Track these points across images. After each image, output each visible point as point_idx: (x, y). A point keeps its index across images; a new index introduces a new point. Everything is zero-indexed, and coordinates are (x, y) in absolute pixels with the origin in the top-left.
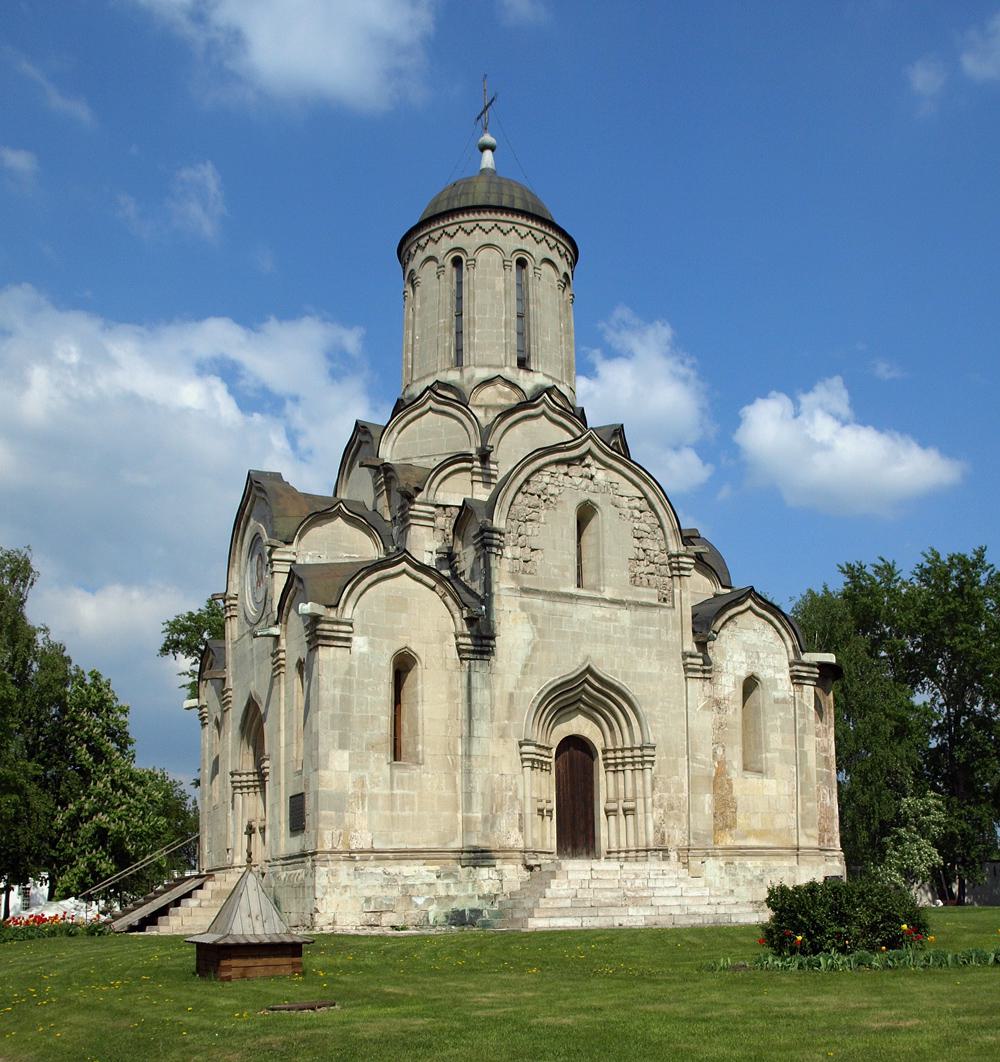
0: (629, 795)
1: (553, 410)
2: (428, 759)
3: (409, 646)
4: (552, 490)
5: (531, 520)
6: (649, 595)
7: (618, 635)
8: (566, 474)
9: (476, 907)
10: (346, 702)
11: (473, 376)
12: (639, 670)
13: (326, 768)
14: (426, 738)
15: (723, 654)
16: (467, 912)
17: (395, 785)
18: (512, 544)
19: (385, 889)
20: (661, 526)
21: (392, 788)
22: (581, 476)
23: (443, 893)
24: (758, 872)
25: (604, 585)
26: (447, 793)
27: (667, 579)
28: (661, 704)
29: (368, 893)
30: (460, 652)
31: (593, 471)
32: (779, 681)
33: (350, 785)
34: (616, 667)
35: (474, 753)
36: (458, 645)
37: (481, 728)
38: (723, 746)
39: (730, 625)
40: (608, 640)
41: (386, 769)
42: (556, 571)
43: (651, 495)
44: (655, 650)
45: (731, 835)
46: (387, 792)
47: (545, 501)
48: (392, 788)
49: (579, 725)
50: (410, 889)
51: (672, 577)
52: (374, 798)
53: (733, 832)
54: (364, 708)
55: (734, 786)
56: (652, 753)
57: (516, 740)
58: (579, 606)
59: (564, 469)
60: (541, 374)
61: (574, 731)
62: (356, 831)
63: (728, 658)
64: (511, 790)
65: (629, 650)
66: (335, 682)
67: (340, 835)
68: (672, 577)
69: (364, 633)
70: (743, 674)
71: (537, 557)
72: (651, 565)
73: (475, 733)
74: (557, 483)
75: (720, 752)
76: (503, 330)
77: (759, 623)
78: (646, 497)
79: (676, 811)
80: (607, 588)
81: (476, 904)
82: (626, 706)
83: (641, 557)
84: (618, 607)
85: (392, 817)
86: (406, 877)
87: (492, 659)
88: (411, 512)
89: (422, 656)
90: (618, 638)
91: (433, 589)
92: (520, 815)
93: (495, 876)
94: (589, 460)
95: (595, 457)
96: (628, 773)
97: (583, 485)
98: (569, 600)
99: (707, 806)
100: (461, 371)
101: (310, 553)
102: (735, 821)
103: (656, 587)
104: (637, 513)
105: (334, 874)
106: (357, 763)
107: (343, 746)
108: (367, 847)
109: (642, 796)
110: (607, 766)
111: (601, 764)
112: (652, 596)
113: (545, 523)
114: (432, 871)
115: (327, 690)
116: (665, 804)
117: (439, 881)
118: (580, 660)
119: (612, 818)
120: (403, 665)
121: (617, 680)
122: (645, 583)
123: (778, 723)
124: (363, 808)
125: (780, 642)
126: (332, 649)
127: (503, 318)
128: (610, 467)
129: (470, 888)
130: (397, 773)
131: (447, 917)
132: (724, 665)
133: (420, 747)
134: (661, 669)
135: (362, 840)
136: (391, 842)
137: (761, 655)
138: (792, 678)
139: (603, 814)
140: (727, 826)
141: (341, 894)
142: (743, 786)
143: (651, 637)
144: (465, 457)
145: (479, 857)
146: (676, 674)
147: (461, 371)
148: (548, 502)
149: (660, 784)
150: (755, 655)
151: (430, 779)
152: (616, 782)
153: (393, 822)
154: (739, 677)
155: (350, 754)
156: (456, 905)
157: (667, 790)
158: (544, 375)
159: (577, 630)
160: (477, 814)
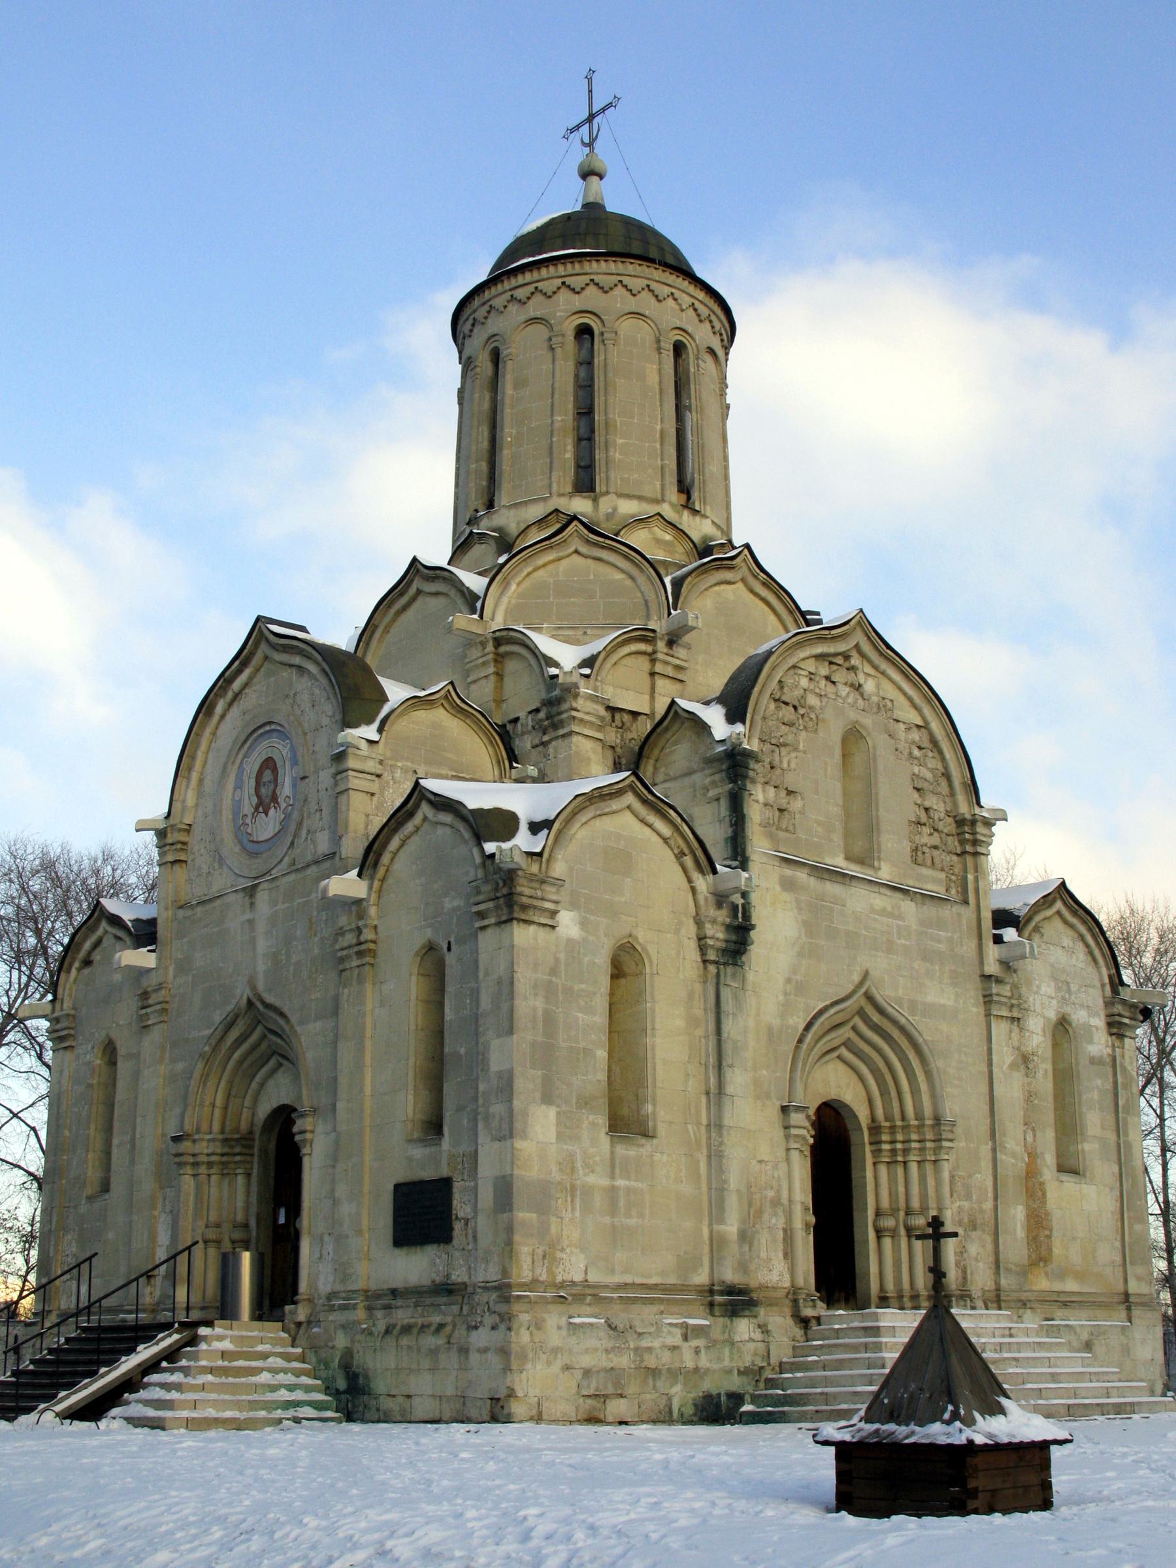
0: (915, 1204)
1: (756, 577)
2: (662, 1129)
3: (634, 932)
4: (812, 700)
5: (785, 745)
6: (932, 881)
7: (903, 941)
8: (827, 678)
9: (734, 1389)
10: (549, 1021)
11: (615, 509)
12: (930, 999)
13: (524, 1136)
14: (659, 1092)
15: (1029, 983)
16: (723, 1398)
17: (617, 1171)
18: (763, 780)
19: (611, 1355)
20: (947, 775)
21: (613, 1177)
22: (846, 684)
23: (689, 1361)
24: (1085, 1336)
25: (879, 859)
26: (686, 1188)
27: (955, 858)
28: (956, 1056)
29: (587, 1361)
30: (703, 949)
31: (861, 678)
32: (1094, 1030)
33: (554, 1168)
34: (901, 992)
35: (727, 1121)
36: (701, 938)
37: (738, 1080)
38: (1033, 1130)
40: (890, 948)
41: (604, 1141)
42: (820, 829)
43: (935, 726)
45: (1047, 1274)
46: (605, 1182)
47: (803, 716)
48: (613, 1177)
49: (837, 1082)
50: (646, 1356)
51: (964, 853)
52: (588, 1191)
53: (1048, 1269)
54: (573, 1033)
55: (1049, 1195)
56: (950, 1136)
57: (778, 1104)
58: (853, 890)
59: (824, 670)
60: (708, 522)
61: (832, 1094)
62: (563, 1250)
63: (1035, 989)
64: (772, 1188)
65: (916, 966)
66: (535, 986)
67: (544, 1256)
68: (964, 853)
69: (573, 906)
70: (1052, 1015)
71: (796, 804)
72: (936, 834)
73: (730, 1089)
74: (817, 690)
75: (1030, 1139)
76: (658, 446)
77: (1067, 938)
78: (924, 727)
79: (979, 1232)
80: (882, 863)
81: (735, 1383)
82: (911, 1055)
83: (924, 818)
84: (899, 895)
85: (613, 1226)
86: (640, 1334)
87: (744, 958)
88: (574, 713)
89: (652, 950)
91: (665, 840)
92: (785, 1230)
93: (758, 1335)
94: (855, 661)
95: (862, 655)
96: (913, 1167)
97: (850, 700)
98: (839, 879)
99: (1019, 1226)
100: (595, 500)
101: (399, 764)
102: (1050, 1250)
103: (942, 870)
104: (916, 752)
105: (539, 1325)
106: (567, 1130)
107: (547, 1098)
108: (578, 1278)
109: (934, 1206)
110: (877, 1153)
111: (868, 1149)
112: (936, 881)
113: (805, 752)
114: (675, 1325)
115: (525, 998)
116: (966, 1220)
117: (686, 1344)
118: (856, 978)
119: (887, 1242)
120: (625, 965)
121: (904, 1016)
122: (929, 862)
123: (1096, 1095)
124: (573, 1210)
125: (1091, 969)
126: (532, 928)
127: (658, 427)
128: (883, 673)
129: (727, 1358)
130: (621, 1150)
131: (696, 1405)
132: (1031, 999)
133: (650, 1108)
134: (956, 1001)
135: (573, 1267)
136: (613, 1272)
137: (1074, 988)
138: (1110, 1025)
139: (872, 1235)
140: (1041, 1259)
141: (549, 1363)
142: (1062, 1194)
143: (942, 947)
144: (646, 636)
145: (735, 1301)
146: (975, 1010)
147: (595, 500)
148: (806, 719)
149: (959, 1186)
150: (1065, 987)
151: (667, 1161)
152: (892, 1181)
153: (615, 1235)
154: (1049, 1019)
155: (558, 1113)
156: (709, 1385)
157: (968, 1196)
158: (713, 522)
159: (851, 928)
160: (731, 1228)
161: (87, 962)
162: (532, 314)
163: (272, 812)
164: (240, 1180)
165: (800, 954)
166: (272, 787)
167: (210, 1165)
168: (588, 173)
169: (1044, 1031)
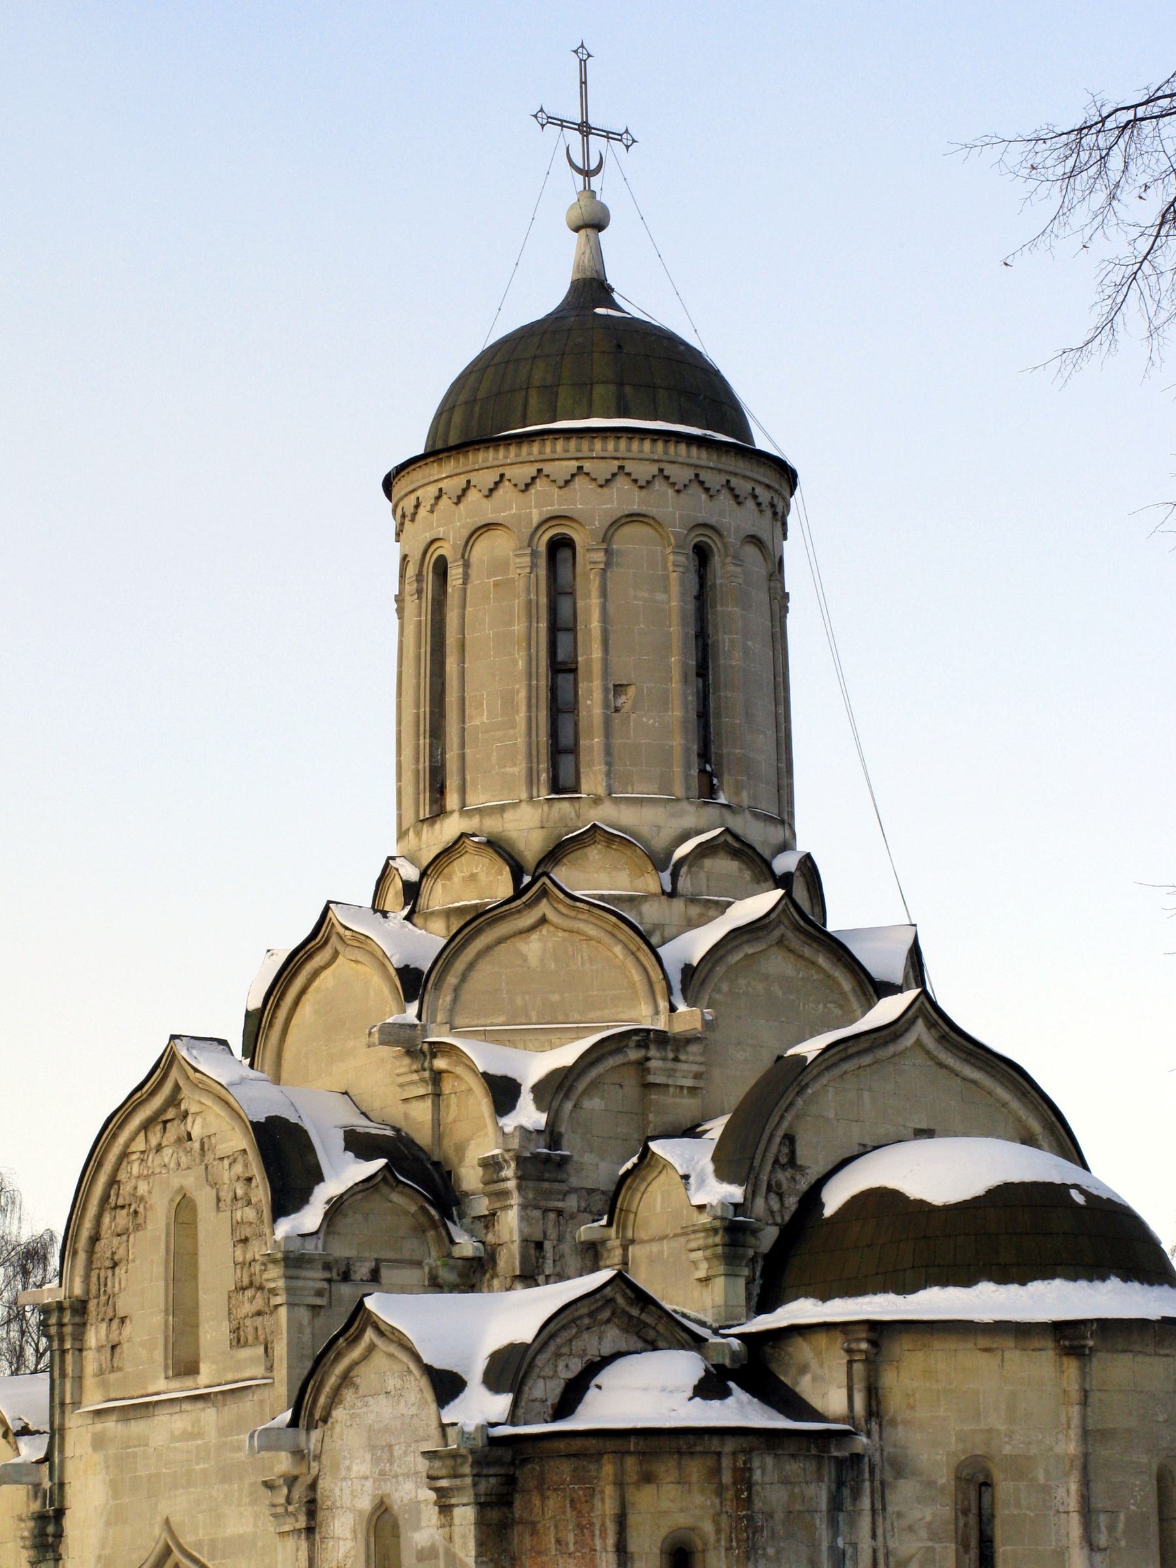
7: (202, 1466)
39: (348, 1395)
44: (247, 1483)
70: (365, 1504)
90: (202, 1470)
98: (143, 1412)
132: (337, 1492)
134: (255, 1525)
154: (360, 1512)
159: (153, 1471)
165: (108, 1524)
169: (355, 1531)
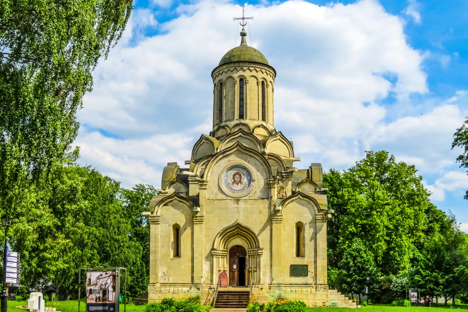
161: (165, 205)
162: (253, 74)
163: (239, 184)
164: (225, 259)
166: (239, 179)
167: (219, 255)
168: (243, 35)
